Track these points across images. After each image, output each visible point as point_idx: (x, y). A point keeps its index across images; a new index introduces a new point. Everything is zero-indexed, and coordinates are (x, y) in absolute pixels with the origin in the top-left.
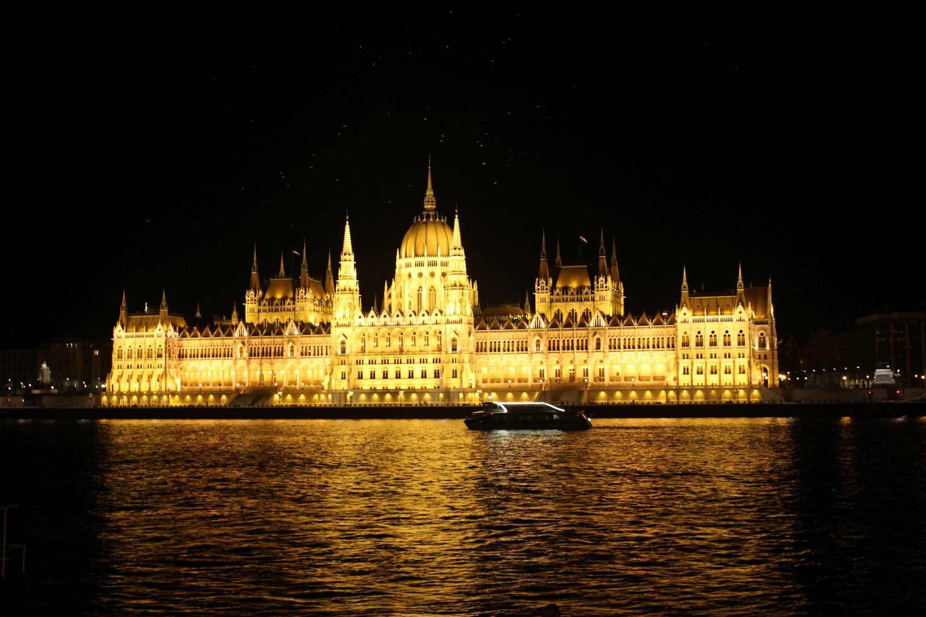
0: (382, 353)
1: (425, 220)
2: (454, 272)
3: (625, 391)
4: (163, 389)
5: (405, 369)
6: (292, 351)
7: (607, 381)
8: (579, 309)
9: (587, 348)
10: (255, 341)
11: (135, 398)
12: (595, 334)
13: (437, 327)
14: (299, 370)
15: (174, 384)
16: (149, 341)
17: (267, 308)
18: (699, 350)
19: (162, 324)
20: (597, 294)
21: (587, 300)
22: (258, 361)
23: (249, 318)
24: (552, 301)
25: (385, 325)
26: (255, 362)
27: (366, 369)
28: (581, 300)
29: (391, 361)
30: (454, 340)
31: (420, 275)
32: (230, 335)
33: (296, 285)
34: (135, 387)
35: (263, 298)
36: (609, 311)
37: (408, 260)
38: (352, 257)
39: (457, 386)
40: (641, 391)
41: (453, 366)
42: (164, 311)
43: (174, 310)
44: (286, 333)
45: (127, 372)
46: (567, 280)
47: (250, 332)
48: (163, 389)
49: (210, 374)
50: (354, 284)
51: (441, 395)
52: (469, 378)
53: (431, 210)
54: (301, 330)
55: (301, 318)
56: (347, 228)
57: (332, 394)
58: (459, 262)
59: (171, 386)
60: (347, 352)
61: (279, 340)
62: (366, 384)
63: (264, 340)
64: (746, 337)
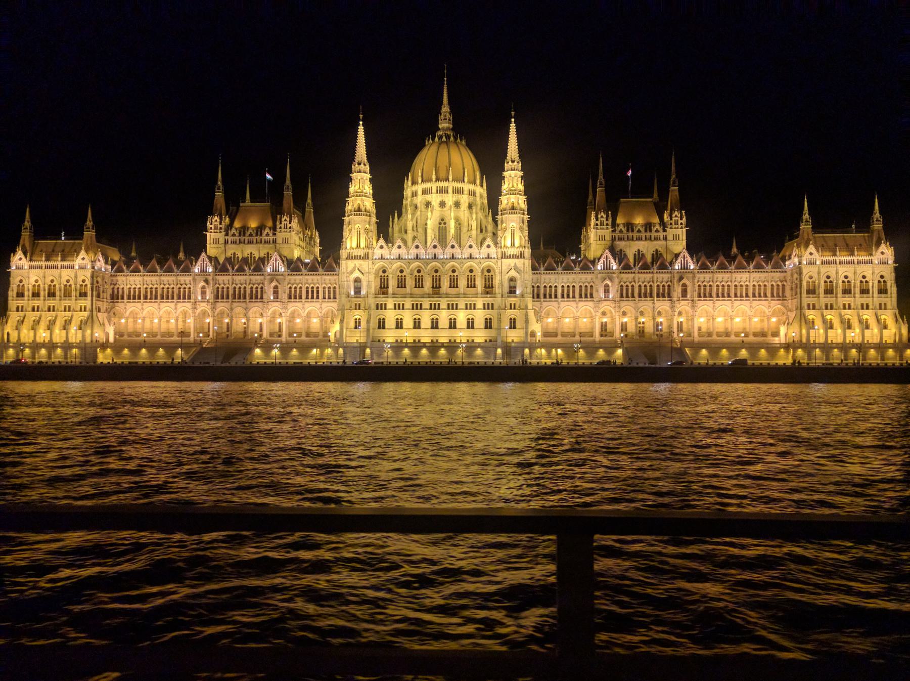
1: (444, 139)
2: (512, 192)
4: (88, 340)
5: (444, 316)
6: (276, 292)
9: (669, 296)
10: (224, 280)
11: (43, 351)
12: (681, 279)
14: (296, 315)
16: (66, 274)
17: (238, 238)
18: (830, 300)
19: (87, 251)
20: (670, 232)
22: (228, 305)
23: (211, 250)
24: (613, 239)
25: (417, 257)
26: (222, 306)
27: (390, 316)
28: (650, 239)
29: (426, 305)
30: (512, 280)
31: (442, 204)
32: (187, 270)
33: (277, 211)
34: (43, 335)
37: (428, 185)
38: (368, 168)
40: (754, 349)
41: (511, 313)
42: (89, 234)
47: (216, 268)
48: (88, 340)
49: (156, 321)
50: (369, 203)
51: (499, 351)
53: (448, 129)
54: (288, 268)
56: (361, 129)
57: (344, 348)
59: (99, 334)
60: (363, 292)
61: (257, 278)
62: (390, 336)
63: (235, 277)
64: (889, 284)
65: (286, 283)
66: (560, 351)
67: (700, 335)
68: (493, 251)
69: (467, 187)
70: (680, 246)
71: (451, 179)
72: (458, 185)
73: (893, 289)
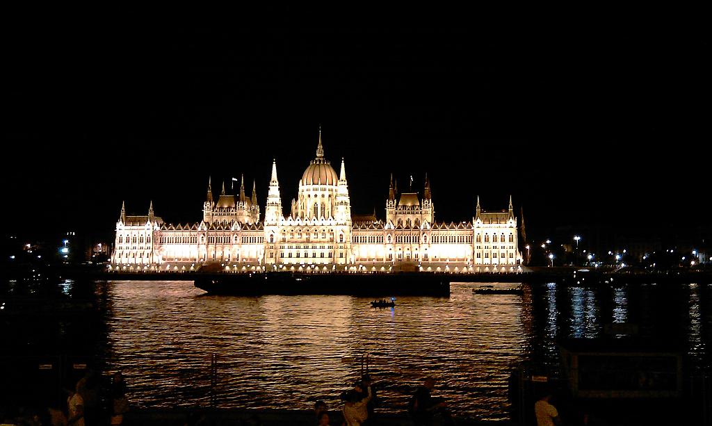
0: (296, 242)
3: (443, 266)
7: (430, 261)
8: (412, 218)
13: (330, 228)
14: (245, 252)
15: (157, 259)
16: (141, 232)
18: (487, 244)
21: (417, 213)
23: (206, 219)
24: (396, 213)
26: (211, 247)
27: (286, 252)
31: (316, 196)
33: (237, 200)
35: (215, 207)
36: (430, 221)
38: (277, 184)
39: (343, 262)
41: (340, 251)
42: (151, 213)
43: (158, 213)
44: (233, 229)
45: (126, 251)
46: (406, 202)
50: (278, 200)
52: (351, 258)
55: (241, 220)
58: (342, 189)
62: (286, 261)
64: (514, 237)
65: (240, 235)
66: (364, 268)
67: (433, 260)
68: (333, 222)
69: (328, 187)
70: (429, 218)
71: (319, 183)
72: (324, 186)
73: (515, 239)
